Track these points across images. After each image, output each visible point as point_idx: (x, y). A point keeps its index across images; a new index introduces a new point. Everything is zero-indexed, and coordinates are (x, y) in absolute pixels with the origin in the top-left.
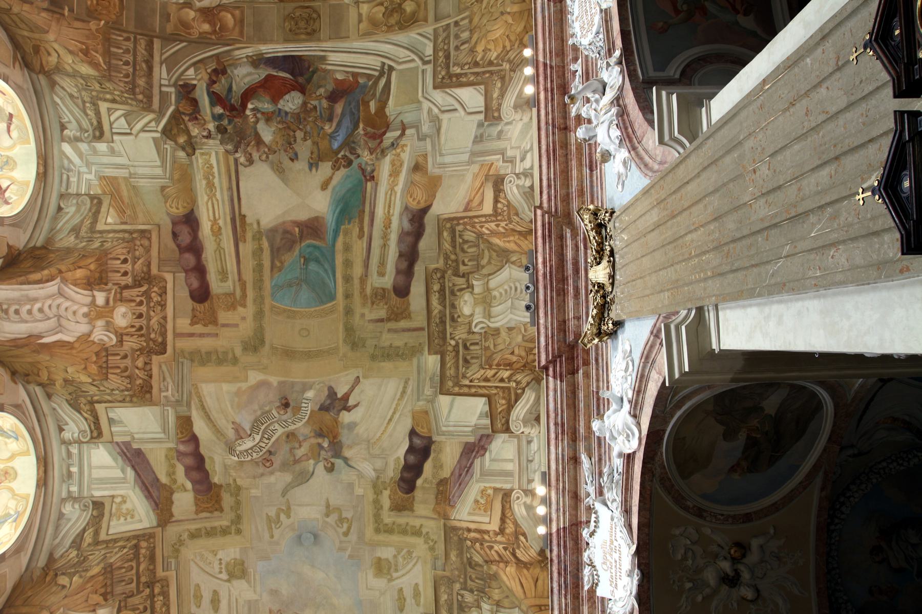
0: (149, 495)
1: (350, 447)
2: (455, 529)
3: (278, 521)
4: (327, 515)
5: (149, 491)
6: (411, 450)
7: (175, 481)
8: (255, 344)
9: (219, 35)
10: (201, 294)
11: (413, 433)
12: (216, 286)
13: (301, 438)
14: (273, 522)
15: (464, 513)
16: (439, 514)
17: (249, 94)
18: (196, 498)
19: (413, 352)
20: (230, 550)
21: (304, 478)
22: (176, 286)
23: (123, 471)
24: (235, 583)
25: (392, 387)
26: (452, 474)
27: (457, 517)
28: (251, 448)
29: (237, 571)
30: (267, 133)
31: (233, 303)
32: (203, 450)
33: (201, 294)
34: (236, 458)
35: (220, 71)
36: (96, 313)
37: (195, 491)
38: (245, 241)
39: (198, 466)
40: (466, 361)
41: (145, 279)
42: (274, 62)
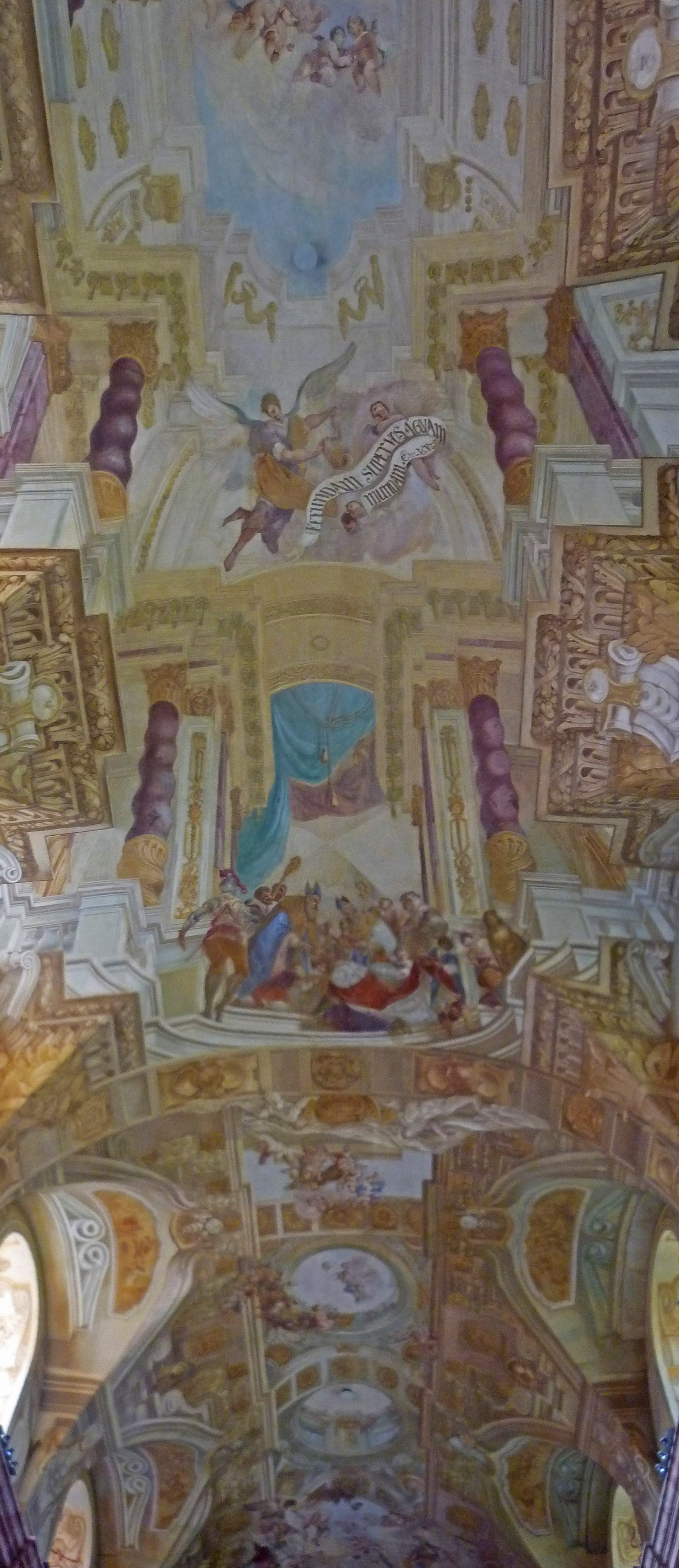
0: (588, 349)
1: (235, 443)
2: (23, 297)
3: (362, 293)
4: (271, 306)
5: (588, 355)
6: (126, 444)
7: (542, 377)
8: (402, 624)
9: (447, 1062)
10: (481, 709)
11: (125, 475)
12: (459, 720)
13: (322, 458)
14: (371, 291)
16: (57, 324)
17: (411, 985)
18: (506, 343)
19: (132, 618)
21: (315, 383)
23: (631, 399)
24: (443, 158)
25: (167, 556)
26: (48, 401)
27: (22, 320)
28: (408, 439)
30: (382, 934)
31: (432, 694)
32: (490, 436)
33: (481, 709)
34: (434, 420)
35: (447, 1017)
37: (505, 358)
38: (414, 787)
39: (500, 406)
40: (35, 612)
41: (563, 741)
42: (375, 1025)
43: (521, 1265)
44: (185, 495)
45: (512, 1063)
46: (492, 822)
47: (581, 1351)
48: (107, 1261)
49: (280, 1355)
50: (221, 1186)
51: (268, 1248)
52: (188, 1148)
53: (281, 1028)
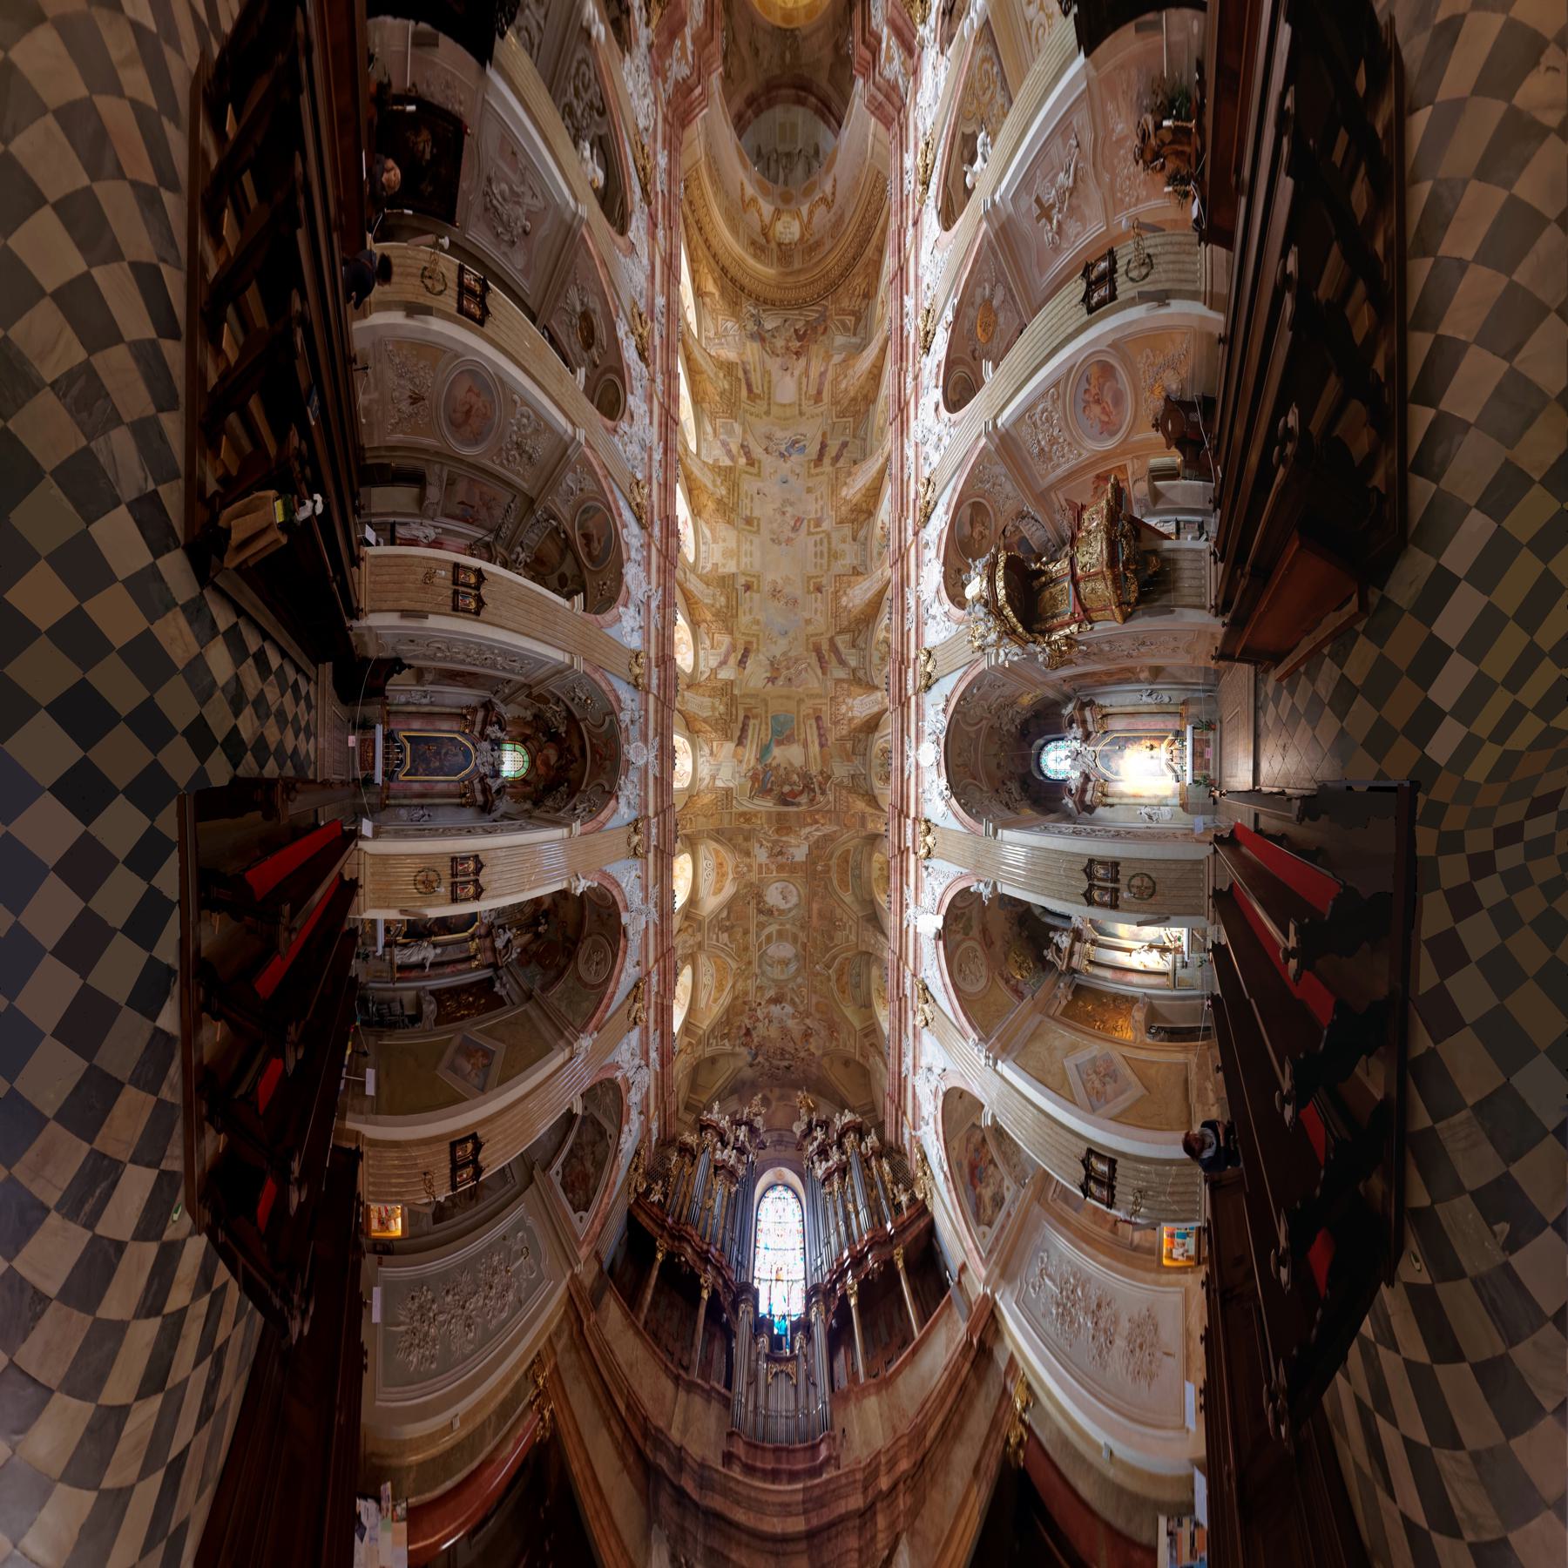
8: (800, 701)
9: (812, 814)
10: (818, 719)
12: (813, 722)
14: (796, 639)
15: (725, 640)
17: (802, 792)
19: (743, 696)
20: (811, 629)
21: (784, 654)
22: (827, 723)
25: (751, 684)
29: (808, 622)
30: (795, 777)
33: (818, 719)
35: (812, 800)
36: (851, 709)
39: (820, 658)
41: (836, 723)
42: (793, 804)
43: (835, 882)
44: (756, 674)
45: (829, 811)
46: (822, 746)
47: (856, 907)
48: (713, 877)
49: (761, 926)
50: (748, 854)
51: (761, 880)
52: (740, 839)
53: (766, 805)
